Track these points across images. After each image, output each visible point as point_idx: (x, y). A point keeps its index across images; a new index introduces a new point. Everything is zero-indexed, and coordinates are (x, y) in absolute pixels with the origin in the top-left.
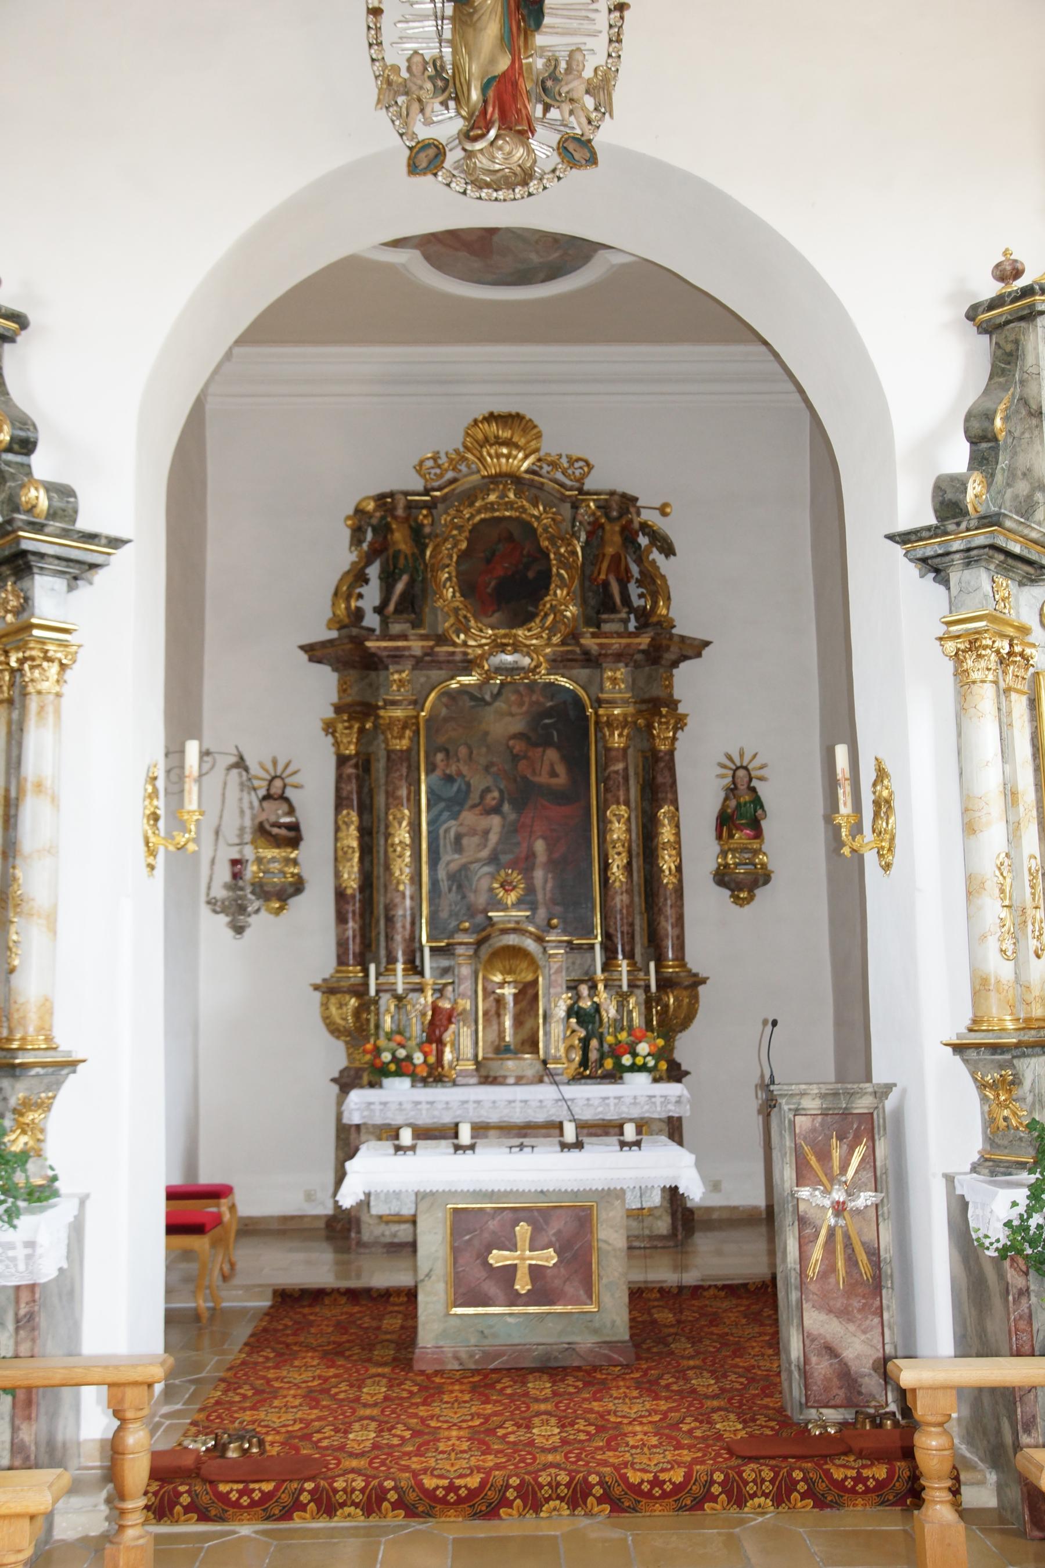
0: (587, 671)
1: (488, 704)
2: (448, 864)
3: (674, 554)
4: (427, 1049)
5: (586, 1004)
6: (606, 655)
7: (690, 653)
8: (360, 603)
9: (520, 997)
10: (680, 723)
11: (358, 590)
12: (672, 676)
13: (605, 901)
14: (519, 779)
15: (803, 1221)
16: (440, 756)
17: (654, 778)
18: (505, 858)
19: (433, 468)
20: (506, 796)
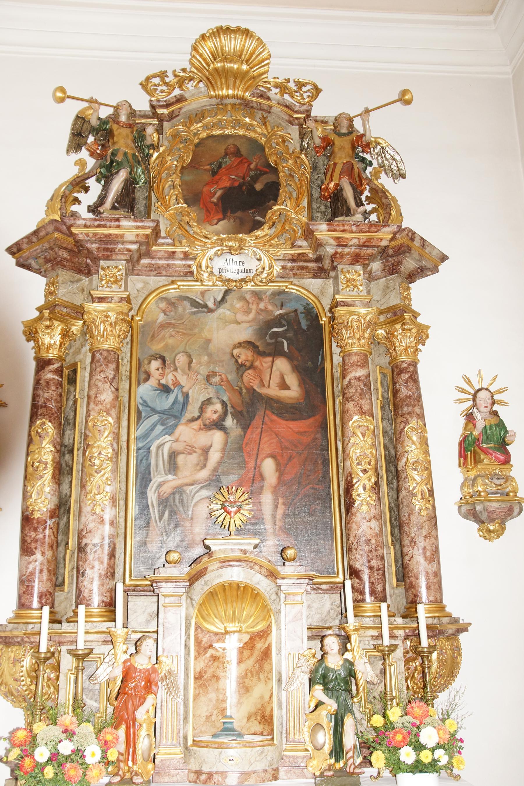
0: (319, 282)
1: (211, 311)
2: (160, 485)
3: (403, 176)
4: (109, 737)
5: (334, 662)
6: (342, 256)
7: (429, 265)
8: (75, 208)
9: (246, 653)
10: (422, 334)
11: (76, 195)
12: (408, 288)
13: (348, 529)
14: (244, 390)
16: (155, 364)
17: (395, 392)
18: (227, 480)
19: (159, 85)
20: (229, 409)
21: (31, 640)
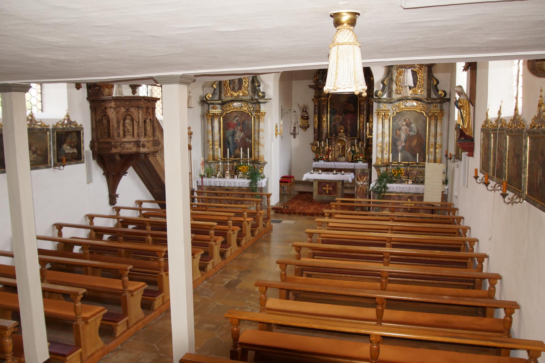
15: (357, 186)
21: (317, 145)
